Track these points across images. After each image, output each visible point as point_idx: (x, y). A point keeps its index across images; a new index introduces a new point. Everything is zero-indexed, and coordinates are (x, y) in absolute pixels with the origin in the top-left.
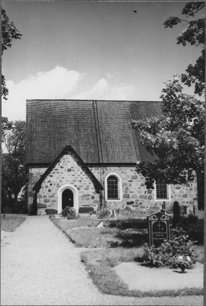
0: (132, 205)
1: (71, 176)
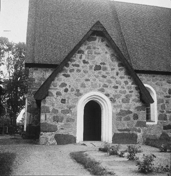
1: (101, 78)
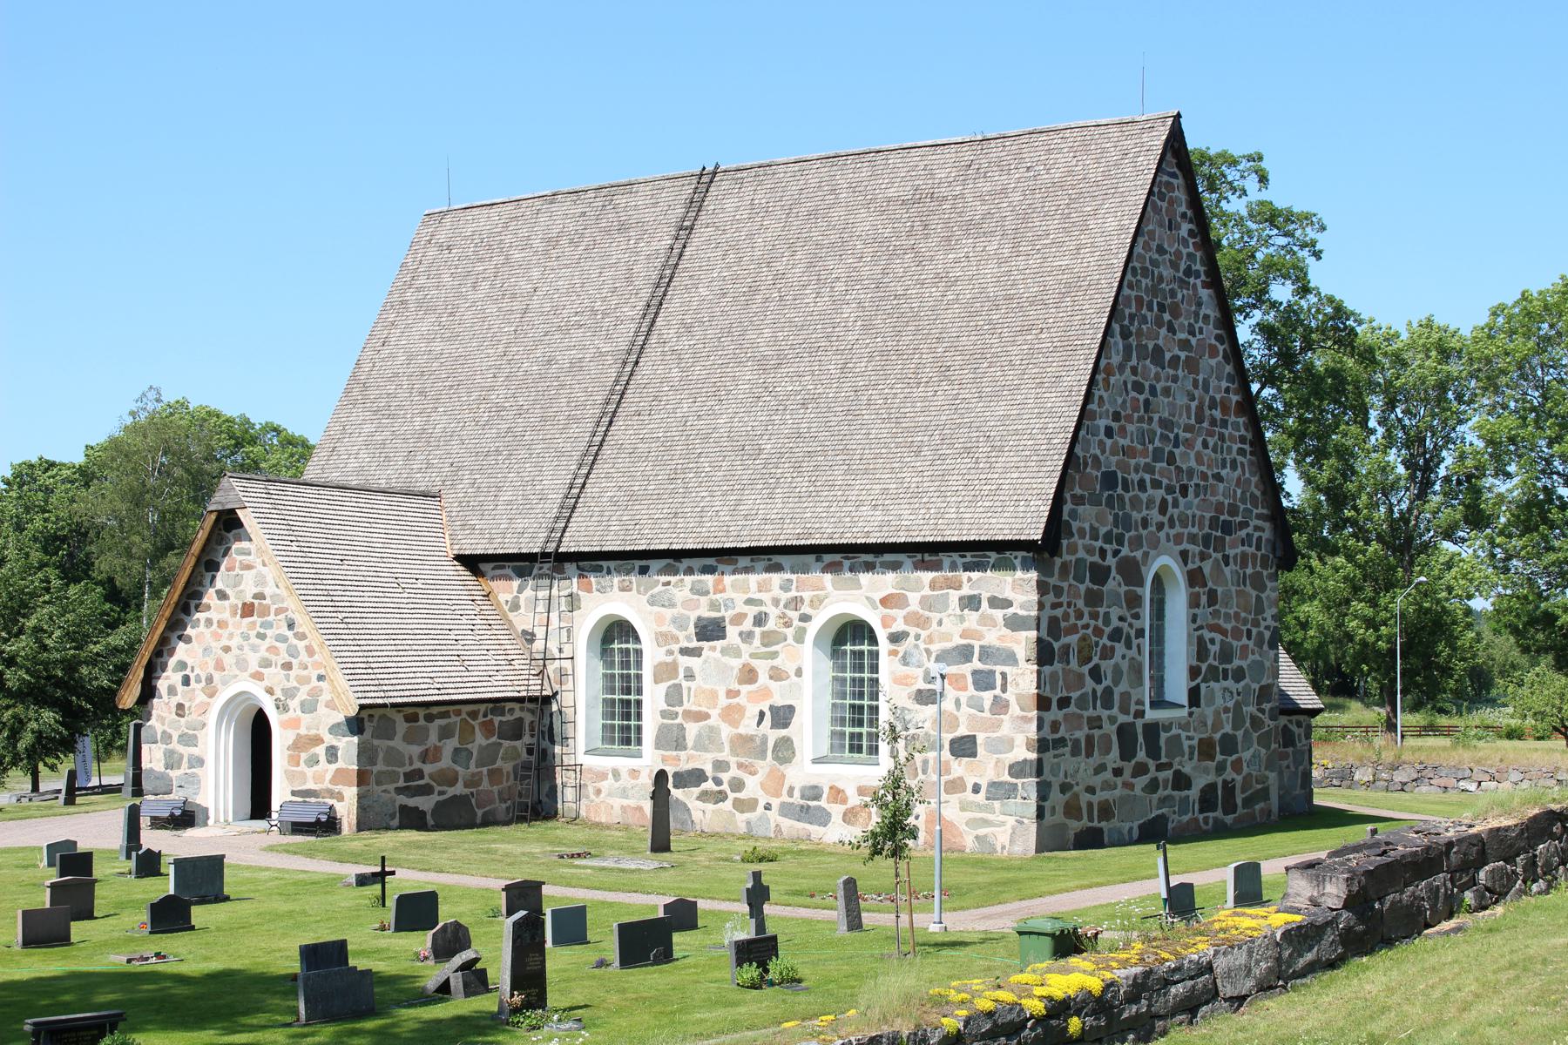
0: (696, 791)
